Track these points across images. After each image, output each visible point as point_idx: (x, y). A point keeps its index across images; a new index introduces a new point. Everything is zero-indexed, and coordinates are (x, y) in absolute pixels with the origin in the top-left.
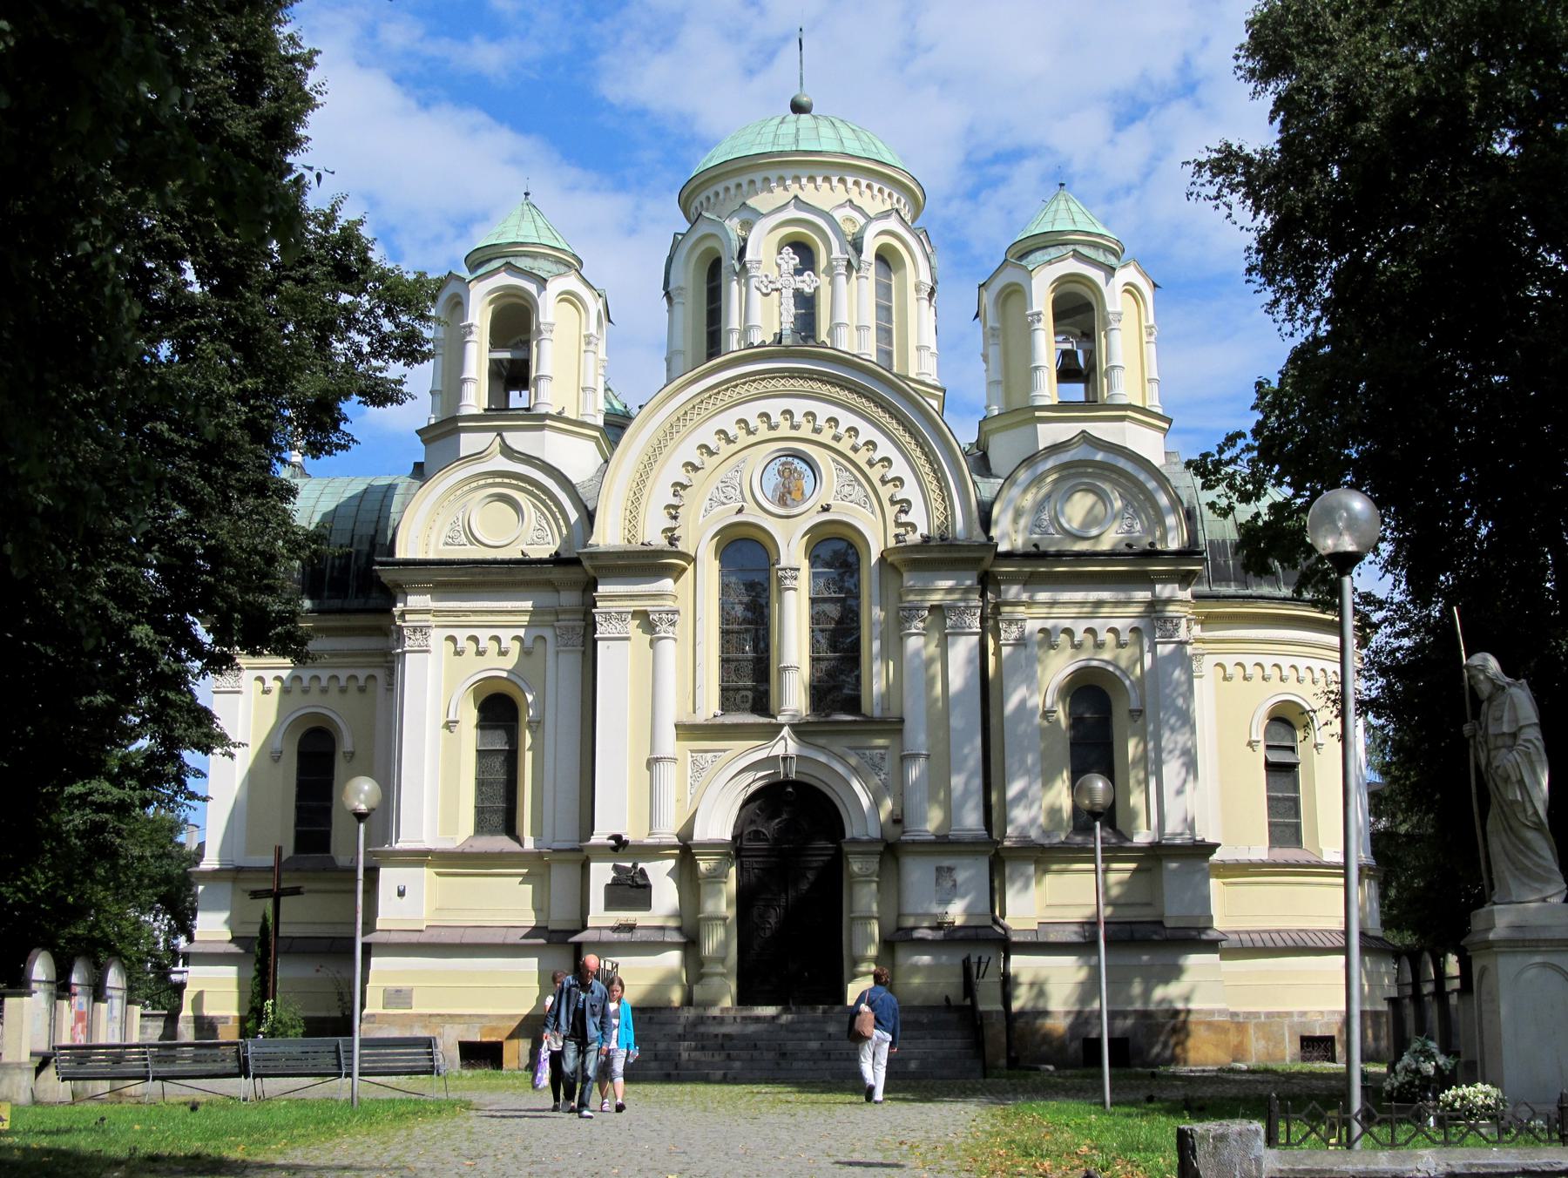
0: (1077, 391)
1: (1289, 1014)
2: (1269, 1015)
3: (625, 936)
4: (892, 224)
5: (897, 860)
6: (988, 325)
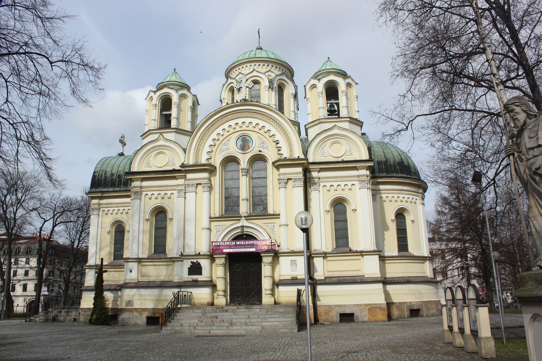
1: (406, 303)
2: (400, 303)
3: (194, 283)
5: (278, 258)
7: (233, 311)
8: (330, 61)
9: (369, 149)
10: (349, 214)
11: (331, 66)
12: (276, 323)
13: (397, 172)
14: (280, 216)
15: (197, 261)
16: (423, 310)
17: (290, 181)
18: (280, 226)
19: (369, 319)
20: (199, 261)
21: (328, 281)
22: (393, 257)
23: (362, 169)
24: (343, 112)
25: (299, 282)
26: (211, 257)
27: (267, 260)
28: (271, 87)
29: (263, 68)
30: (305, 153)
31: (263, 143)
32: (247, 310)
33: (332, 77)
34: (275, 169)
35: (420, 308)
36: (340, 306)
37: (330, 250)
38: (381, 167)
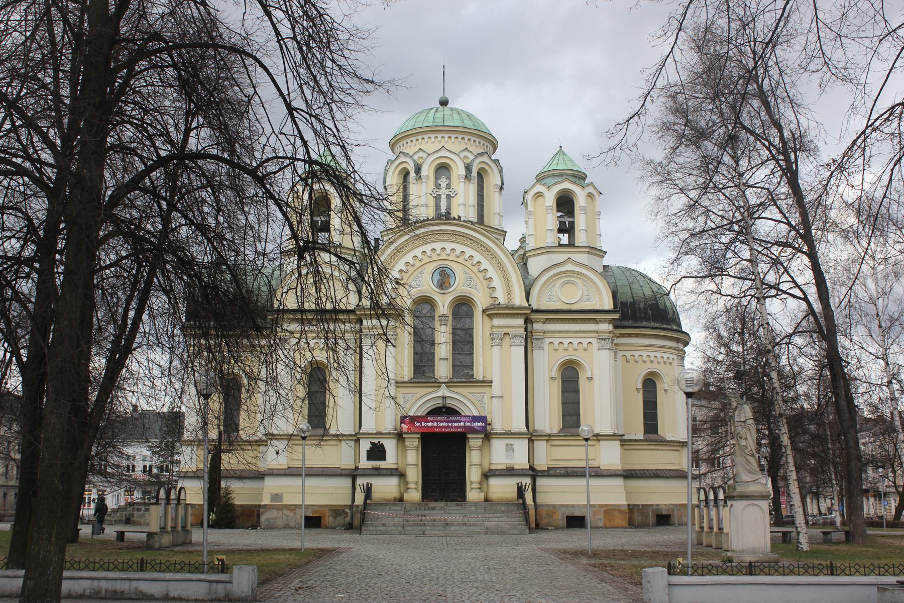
0: (565, 239)
1: (652, 505)
2: (643, 505)
3: (375, 472)
4: (485, 159)
5: (489, 440)
6: (529, 209)
7: (442, 508)
8: (564, 154)
9: (615, 295)
10: (583, 384)
11: (566, 165)
12: (501, 524)
13: (648, 320)
14: (493, 384)
15: (379, 442)
16: (674, 516)
17: (507, 337)
18: (492, 397)
19: (605, 524)
20: (382, 441)
21: (551, 473)
22: (636, 441)
23: (602, 322)
24: (581, 239)
25: (517, 472)
26: (400, 436)
27: (474, 442)
28: (468, 177)
29: (455, 145)
30: (528, 299)
31: (470, 279)
32: (459, 508)
33: (567, 185)
34: (486, 318)
35: (671, 513)
36: (567, 506)
37: (555, 431)
38: (625, 311)
